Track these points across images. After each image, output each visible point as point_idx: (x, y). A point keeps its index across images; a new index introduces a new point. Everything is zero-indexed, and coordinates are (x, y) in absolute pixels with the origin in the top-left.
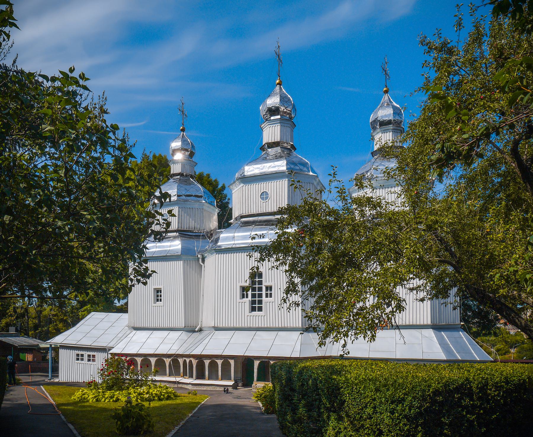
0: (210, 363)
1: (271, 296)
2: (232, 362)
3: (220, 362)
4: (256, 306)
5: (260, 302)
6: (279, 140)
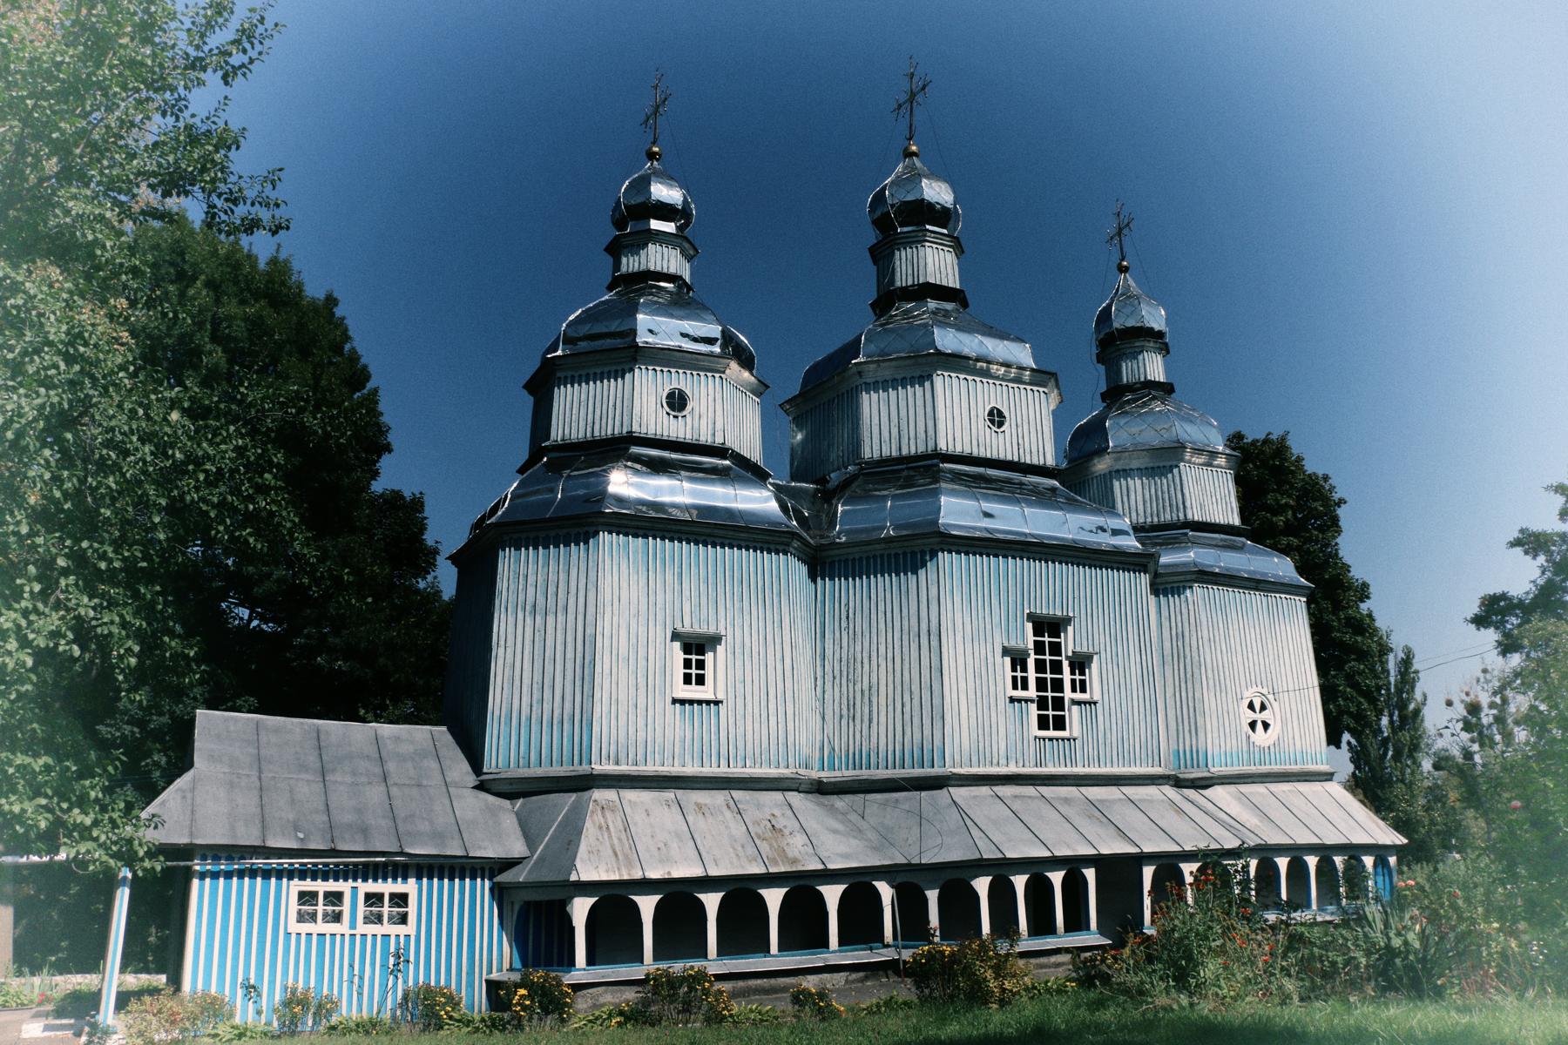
1: (1083, 690)
2: (1090, 874)
5: (1059, 704)
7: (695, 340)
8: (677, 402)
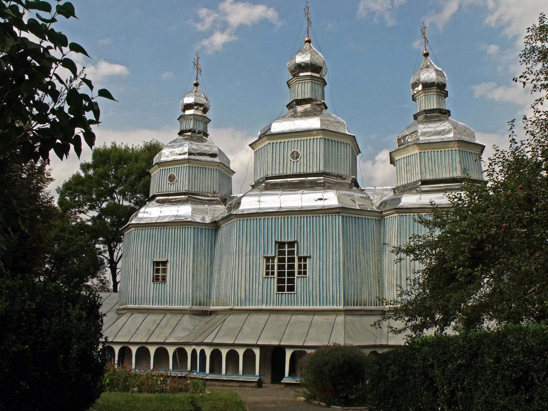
0: (228, 354)
2: (257, 352)
3: (241, 352)
4: (286, 284)
6: (309, 97)
7: (180, 155)
8: (172, 178)
